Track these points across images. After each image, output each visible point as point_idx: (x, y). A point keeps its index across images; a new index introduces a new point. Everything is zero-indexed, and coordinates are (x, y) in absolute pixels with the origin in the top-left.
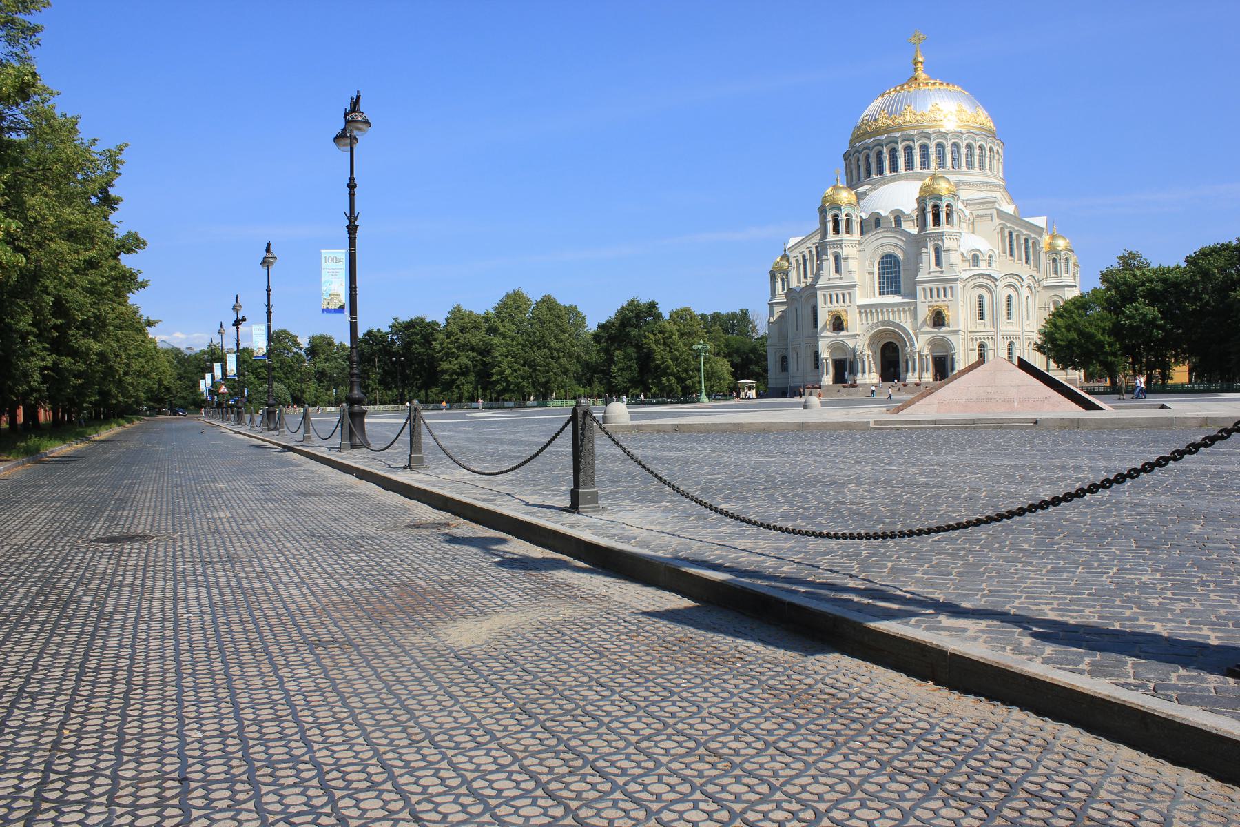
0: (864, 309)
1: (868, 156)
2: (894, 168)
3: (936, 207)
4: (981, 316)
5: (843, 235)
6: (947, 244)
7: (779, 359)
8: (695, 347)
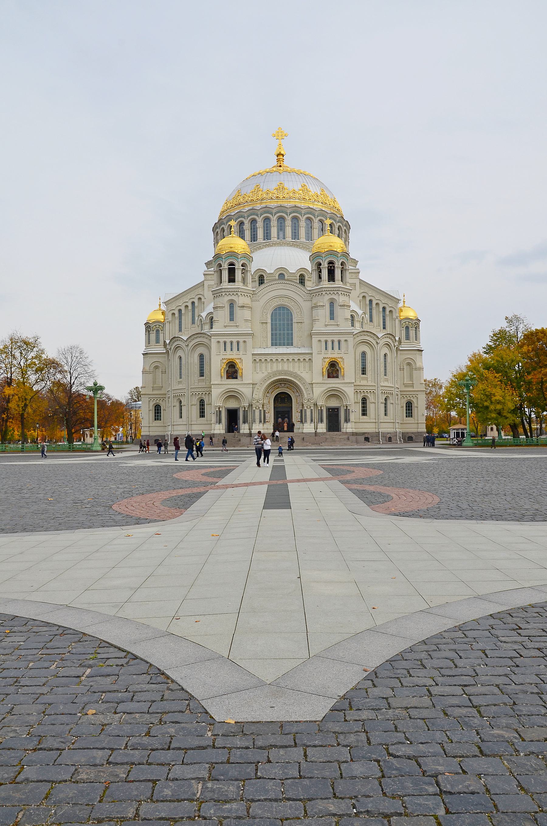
0: (258, 359)
1: (241, 224)
2: (267, 236)
3: (331, 263)
4: (364, 372)
5: (238, 284)
6: (341, 299)
7: (152, 408)
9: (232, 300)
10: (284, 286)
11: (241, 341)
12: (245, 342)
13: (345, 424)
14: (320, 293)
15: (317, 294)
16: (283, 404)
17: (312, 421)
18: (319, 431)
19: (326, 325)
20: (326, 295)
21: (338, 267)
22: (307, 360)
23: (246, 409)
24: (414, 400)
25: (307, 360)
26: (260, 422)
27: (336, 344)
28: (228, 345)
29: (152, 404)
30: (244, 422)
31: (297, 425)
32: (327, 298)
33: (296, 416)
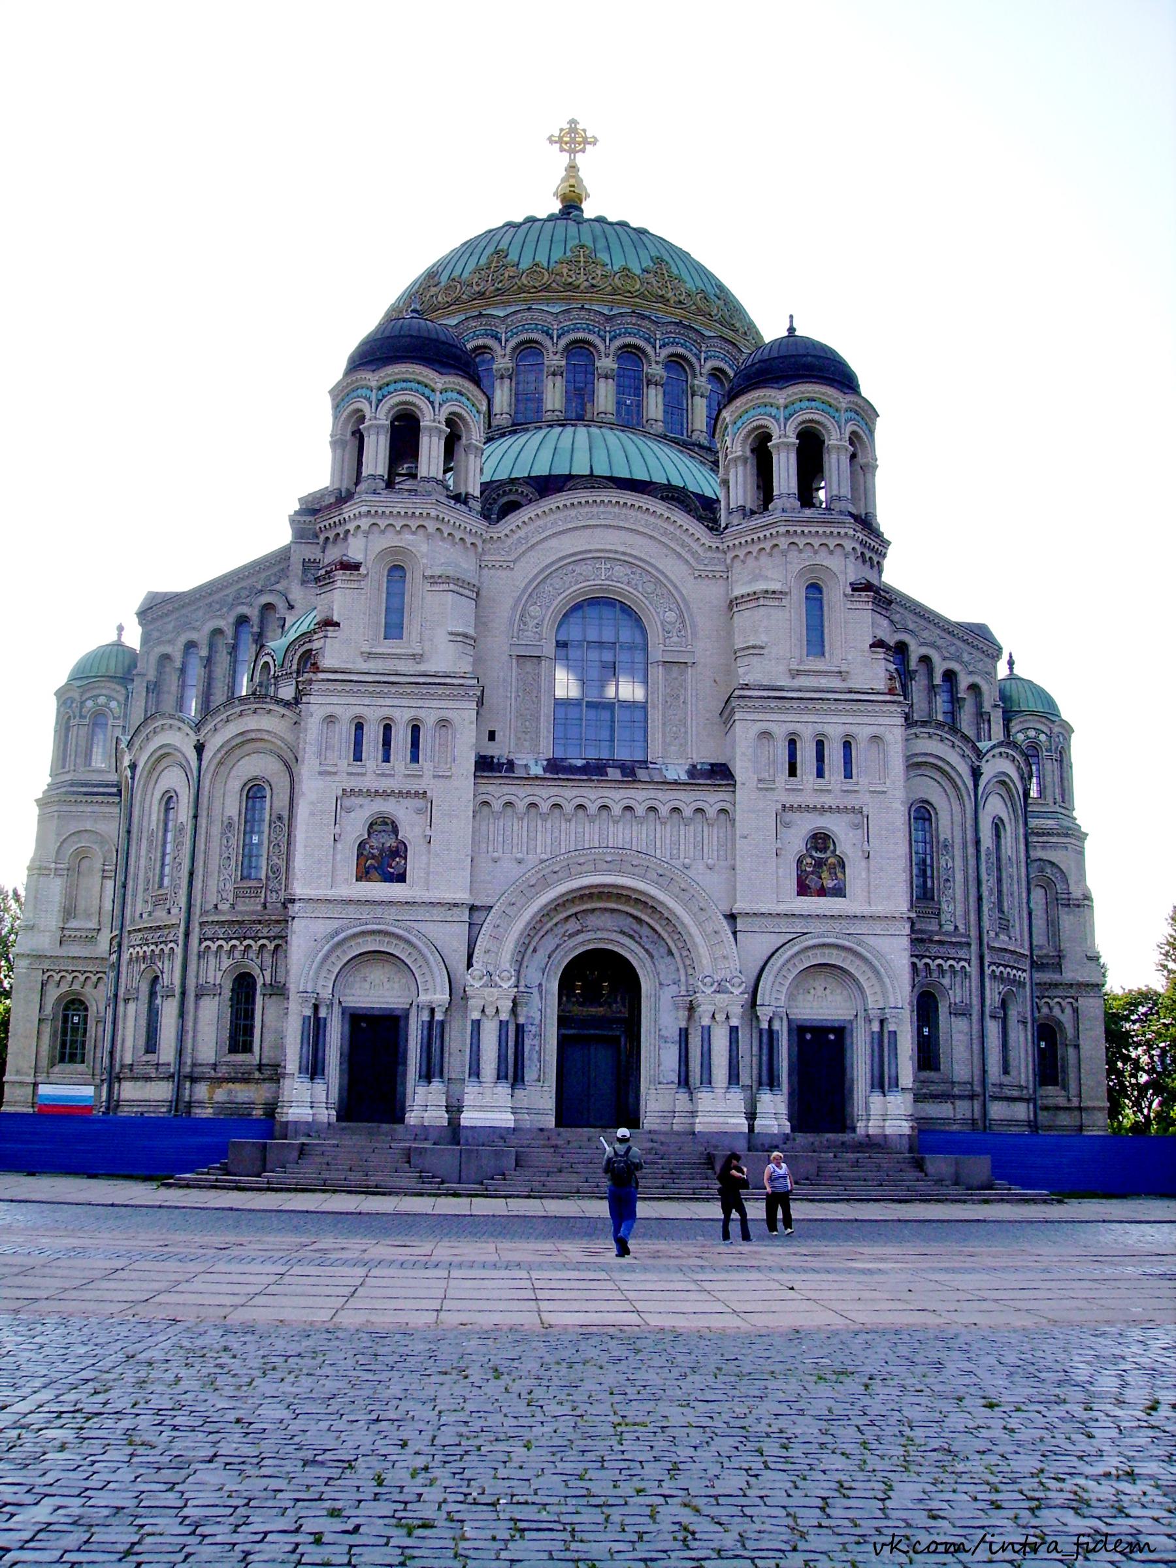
9: (394, 551)
10: (617, 516)
11: (429, 720)
12: (444, 723)
13: (876, 1100)
14: (767, 545)
15: (754, 549)
16: (600, 999)
17: (733, 1077)
19: (795, 674)
20: (793, 554)
21: (838, 448)
22: (711, 812)
23: (439, 1016)
24: (1066, 1018)
25: (711, 812)
26: (501, 1076)
27: (834, 754)
28: (373, 735)
29: (53, 994)
30: (427, 1076)
31: (657, 1101)
32: (798, 562)
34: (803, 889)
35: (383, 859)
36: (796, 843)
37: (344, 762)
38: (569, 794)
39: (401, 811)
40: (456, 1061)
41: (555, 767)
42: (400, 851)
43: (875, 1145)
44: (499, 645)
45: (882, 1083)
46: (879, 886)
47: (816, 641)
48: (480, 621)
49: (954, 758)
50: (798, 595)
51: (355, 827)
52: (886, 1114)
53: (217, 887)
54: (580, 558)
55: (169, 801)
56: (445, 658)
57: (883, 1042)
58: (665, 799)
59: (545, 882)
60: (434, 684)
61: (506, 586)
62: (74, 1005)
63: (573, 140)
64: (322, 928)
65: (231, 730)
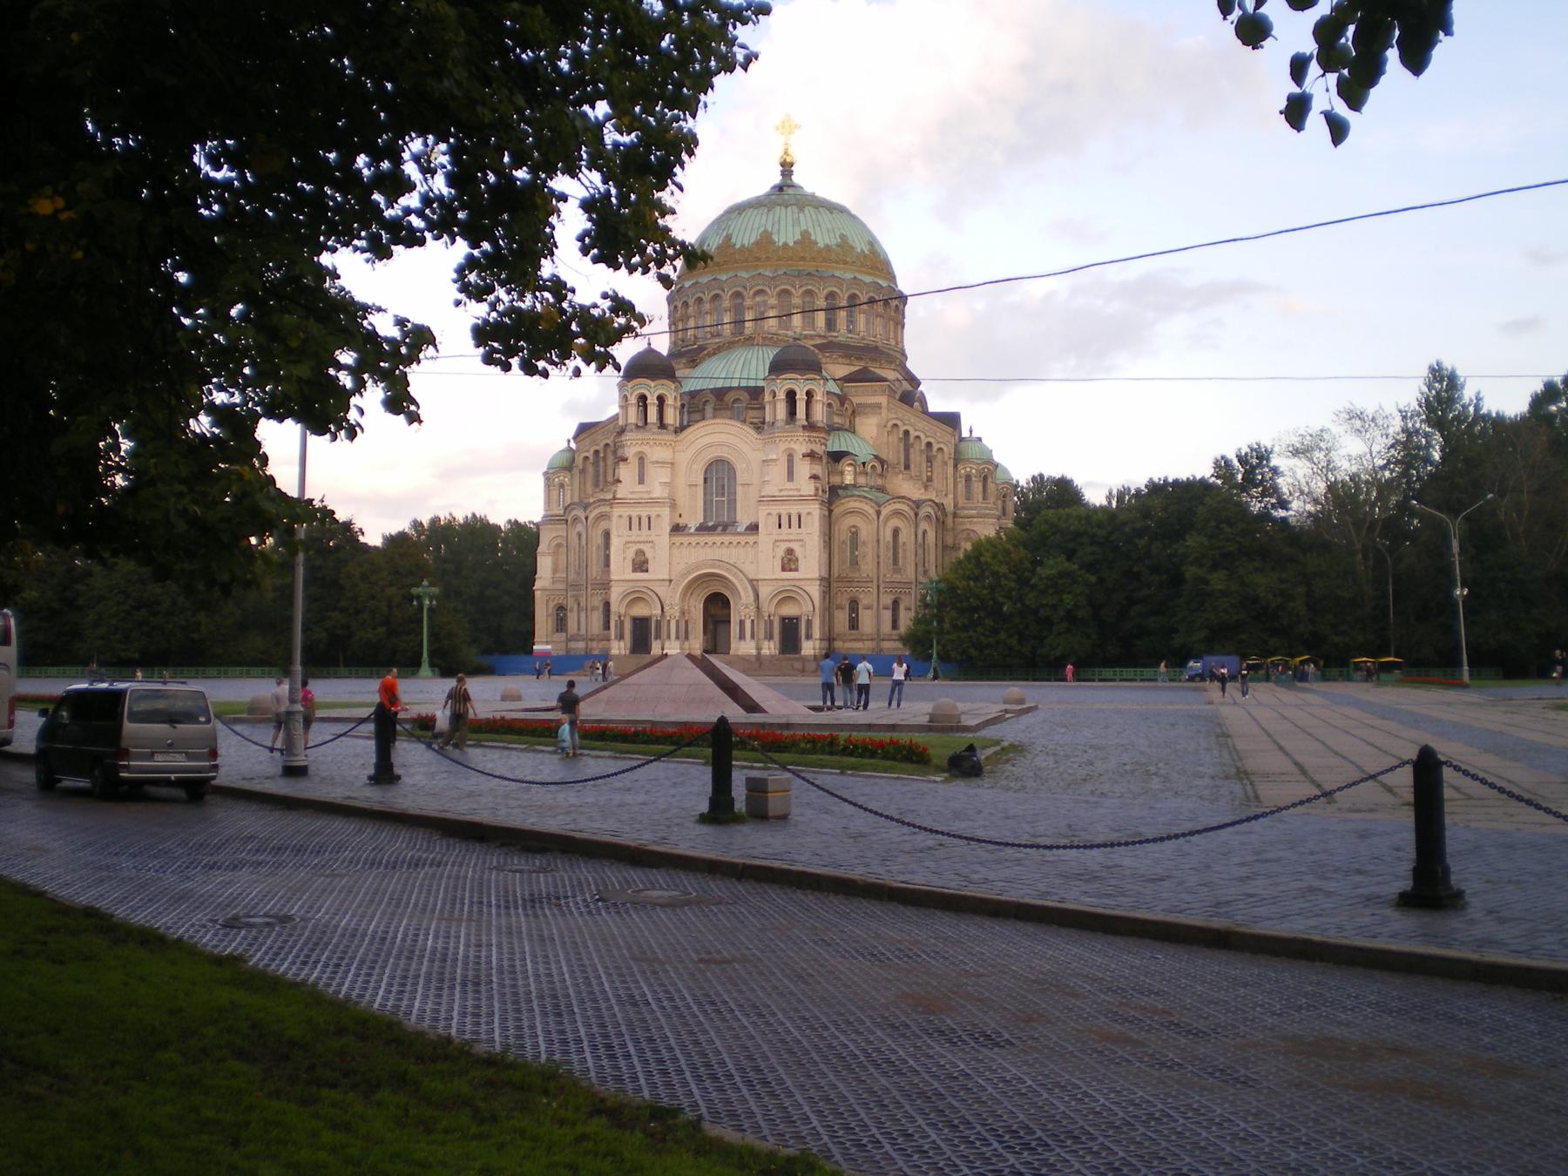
8: (415, 591)
16: (717, 607)
17: (753, 637)
18: (765, 652)
29: (551, 605)
32: (783, 446)
33: (734, 628)
34: (783, 569)
35: (641, 565)
36: (781, 552)
37: (626, 532)
38: (703, 539)
39: (645, 548)
40: (664, 635)
41: (703, 529)
42: (646, 561)
43: (804, 659)
44: (681, 483)
45: (809, 637)
46: (811, 566)
47: (791, 475)
48: (673, 475)
49: (867, 508)
50: (784, 460)
51: (631, 554)
52: (809, 648)
53: (595, 571)
54: (711, 445)
55: (580, 535)
56: (658, 492)
57: (809, 623)
58: (735, 539)
59: (689, 573)
60: (654, 502)
61: (683, 459)
62: (561, 608)
63: (788, 127)
64: (620, 590)
65: (596, 512)
